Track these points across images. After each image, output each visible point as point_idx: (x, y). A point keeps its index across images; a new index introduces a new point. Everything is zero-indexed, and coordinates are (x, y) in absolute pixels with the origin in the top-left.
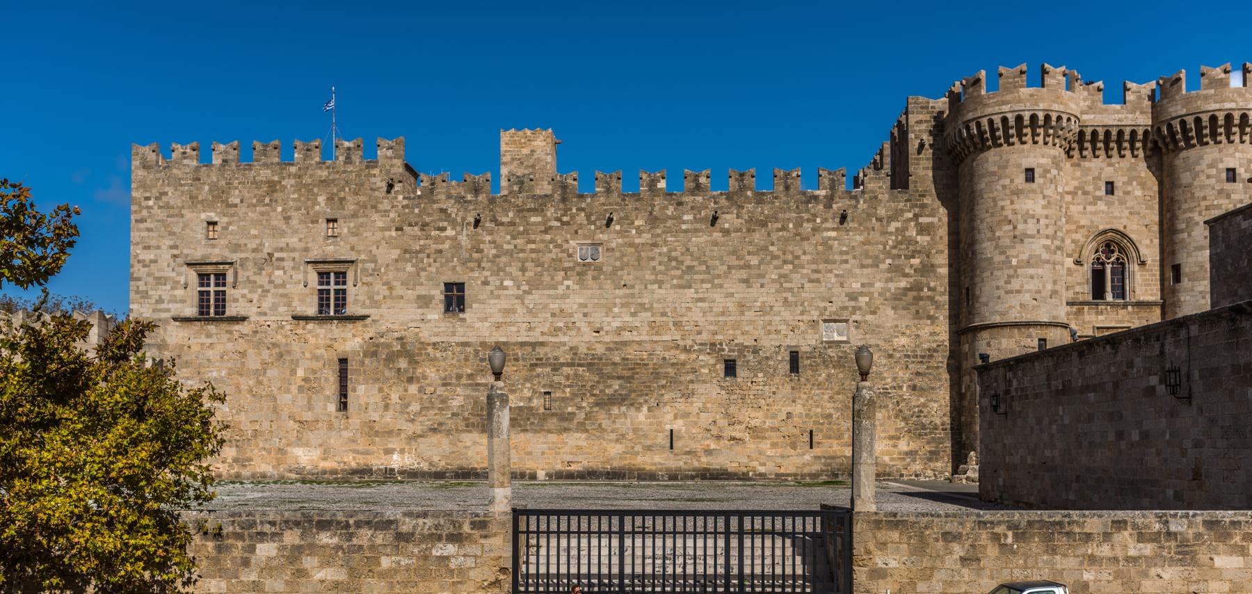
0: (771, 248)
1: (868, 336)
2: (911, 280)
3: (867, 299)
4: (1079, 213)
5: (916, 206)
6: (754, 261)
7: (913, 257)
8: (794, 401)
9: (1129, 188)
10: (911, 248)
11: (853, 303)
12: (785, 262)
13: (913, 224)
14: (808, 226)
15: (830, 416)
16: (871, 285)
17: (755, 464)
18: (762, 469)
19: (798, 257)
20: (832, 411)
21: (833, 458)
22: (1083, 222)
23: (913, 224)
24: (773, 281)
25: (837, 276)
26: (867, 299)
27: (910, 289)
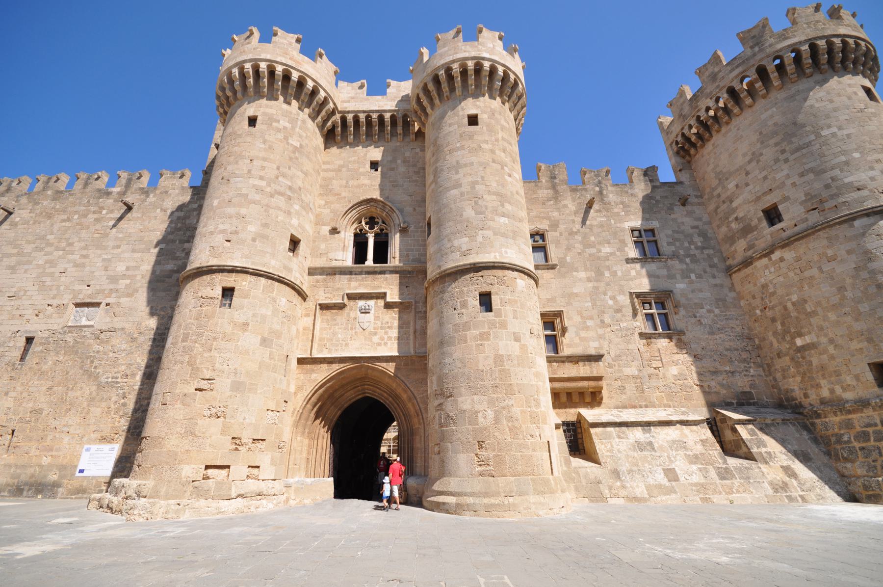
0: (49, 237)
1: (116, 319)
3: (128, 281)
4: (341, 186)
6: (28, 248)
9: (393, 165)
11: (112, 286)
12: (57, 249)
14: (91, 217)
15: (40, 411)
16: (137, 268)
19: (71, 244)
20: (44, 406)
22: (344, 194)
24: (38, 267)
25: (104, 260)
26: (128, 281)
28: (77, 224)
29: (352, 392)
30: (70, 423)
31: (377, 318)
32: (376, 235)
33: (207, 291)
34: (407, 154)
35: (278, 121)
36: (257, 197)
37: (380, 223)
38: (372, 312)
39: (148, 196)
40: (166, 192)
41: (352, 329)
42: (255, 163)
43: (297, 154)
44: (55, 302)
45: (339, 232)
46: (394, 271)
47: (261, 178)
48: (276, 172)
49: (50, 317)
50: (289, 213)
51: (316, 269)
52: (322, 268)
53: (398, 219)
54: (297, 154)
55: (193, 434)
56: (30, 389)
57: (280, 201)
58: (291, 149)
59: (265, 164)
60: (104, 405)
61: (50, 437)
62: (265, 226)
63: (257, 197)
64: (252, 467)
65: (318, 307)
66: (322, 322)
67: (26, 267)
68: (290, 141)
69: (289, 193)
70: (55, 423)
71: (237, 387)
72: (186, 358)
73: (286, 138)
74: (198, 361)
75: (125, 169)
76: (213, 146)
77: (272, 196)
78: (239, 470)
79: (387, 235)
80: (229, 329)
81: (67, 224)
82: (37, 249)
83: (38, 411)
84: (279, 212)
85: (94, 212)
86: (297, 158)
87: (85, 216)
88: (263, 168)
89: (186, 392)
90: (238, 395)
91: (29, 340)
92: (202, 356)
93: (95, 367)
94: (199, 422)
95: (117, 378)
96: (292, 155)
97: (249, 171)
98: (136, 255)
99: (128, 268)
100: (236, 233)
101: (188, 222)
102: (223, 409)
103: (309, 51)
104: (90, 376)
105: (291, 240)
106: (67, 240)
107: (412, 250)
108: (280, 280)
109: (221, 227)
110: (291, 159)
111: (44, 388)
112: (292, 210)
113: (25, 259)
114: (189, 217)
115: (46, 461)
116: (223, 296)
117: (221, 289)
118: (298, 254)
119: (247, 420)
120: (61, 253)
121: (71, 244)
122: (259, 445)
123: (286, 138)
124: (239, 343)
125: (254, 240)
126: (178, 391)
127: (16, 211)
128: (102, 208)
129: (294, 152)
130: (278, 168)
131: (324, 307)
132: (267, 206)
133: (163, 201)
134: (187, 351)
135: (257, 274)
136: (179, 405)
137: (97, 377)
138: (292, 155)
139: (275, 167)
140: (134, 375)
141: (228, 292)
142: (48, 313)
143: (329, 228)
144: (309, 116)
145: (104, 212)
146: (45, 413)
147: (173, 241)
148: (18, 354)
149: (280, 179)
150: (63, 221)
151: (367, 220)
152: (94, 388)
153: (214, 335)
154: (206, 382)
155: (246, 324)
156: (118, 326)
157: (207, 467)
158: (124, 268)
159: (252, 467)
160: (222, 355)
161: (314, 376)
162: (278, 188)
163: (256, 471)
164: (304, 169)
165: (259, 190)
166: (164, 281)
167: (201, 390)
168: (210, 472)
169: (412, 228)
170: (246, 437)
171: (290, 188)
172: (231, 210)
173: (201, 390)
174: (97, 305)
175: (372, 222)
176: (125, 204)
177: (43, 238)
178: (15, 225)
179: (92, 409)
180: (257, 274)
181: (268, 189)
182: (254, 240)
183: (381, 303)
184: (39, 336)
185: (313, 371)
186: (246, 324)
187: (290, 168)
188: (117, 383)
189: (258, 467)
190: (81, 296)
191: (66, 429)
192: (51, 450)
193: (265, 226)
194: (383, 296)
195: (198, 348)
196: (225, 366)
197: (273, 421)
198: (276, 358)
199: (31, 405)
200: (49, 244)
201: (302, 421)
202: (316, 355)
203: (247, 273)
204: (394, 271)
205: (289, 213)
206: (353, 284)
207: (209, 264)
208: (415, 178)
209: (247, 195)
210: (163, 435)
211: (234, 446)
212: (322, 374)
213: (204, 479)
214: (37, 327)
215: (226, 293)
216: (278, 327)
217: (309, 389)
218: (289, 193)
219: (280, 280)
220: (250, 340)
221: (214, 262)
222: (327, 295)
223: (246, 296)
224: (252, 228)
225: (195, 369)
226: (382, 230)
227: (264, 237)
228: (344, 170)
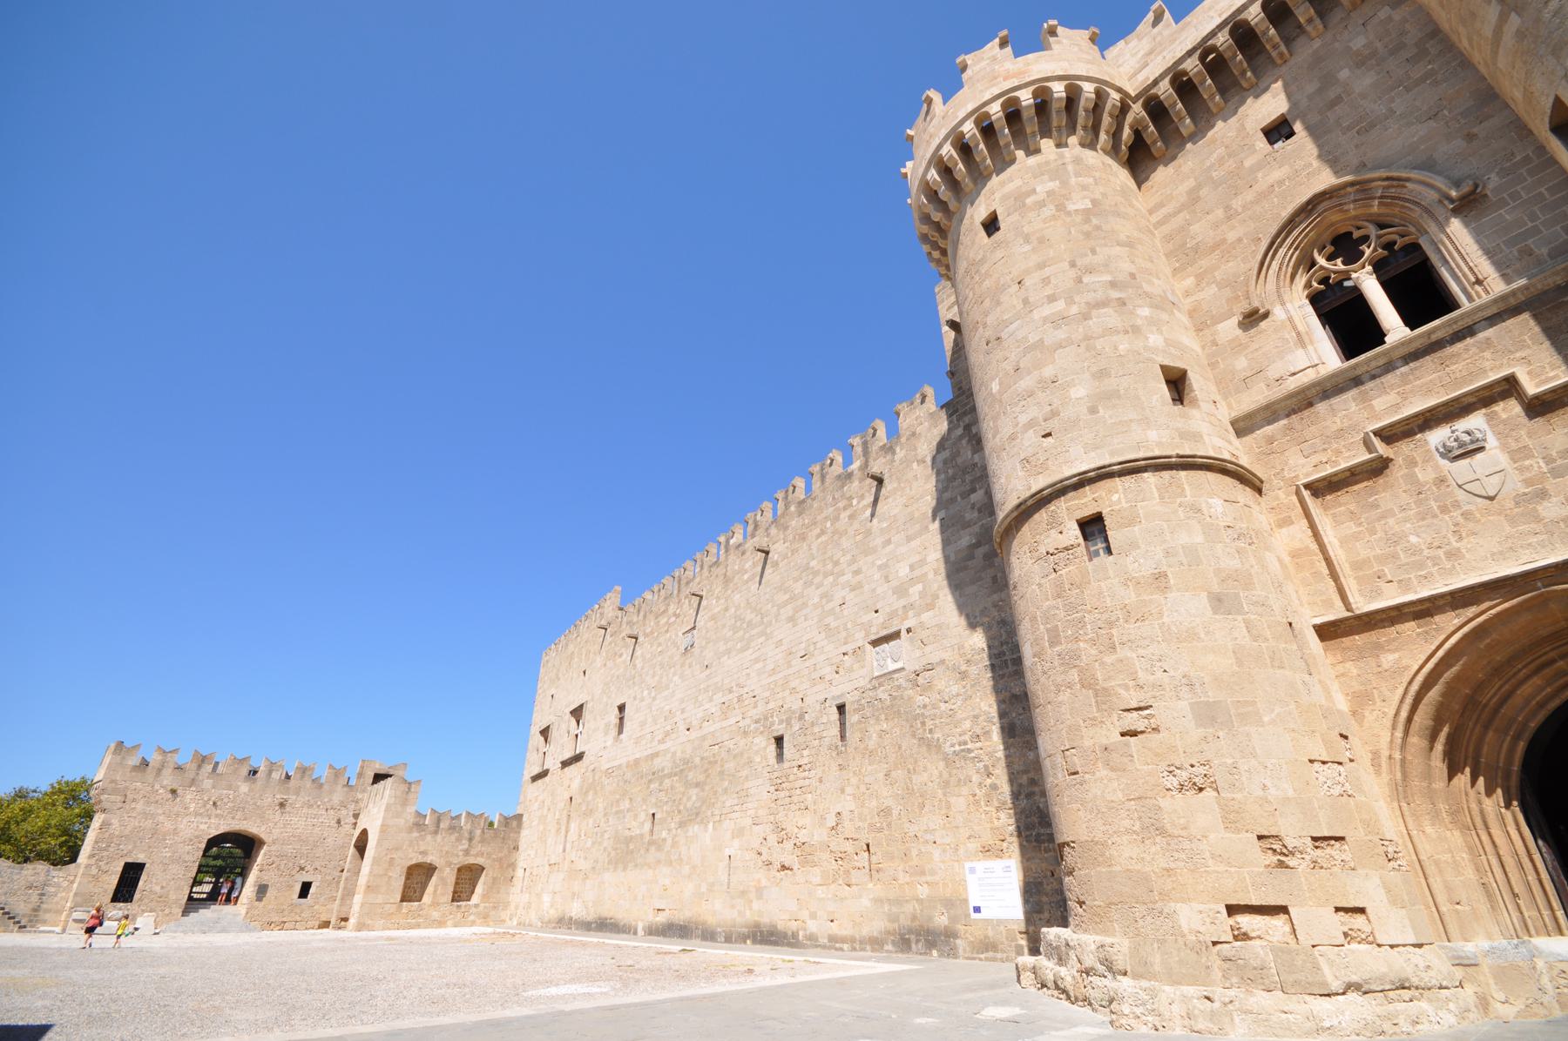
0: (813, 563)
1: (928, 649)
2: (976, 529)
3: (919, 587)
4: (1216, 226)
5: (965, 414)
7: (973, 490)
8: (843, 791)
10: (968, 478)
12: (826, 576)
13: (964, 442)
14: (844, 515)
16: (923, 562)
17: (805, 914)
18: (812, 926)
20: (890, 802)
21: (898, 902)
22: (1231, 236)
23: (964, 442)
25: (880, 567)
26: (919, 587)
27: (978, 545)
28: (834, 533)
29: (1537, 681)
30: (932, 826)
31: (1518, 454)
32: (1379, 267)
33: (1052, 540)
34: (1358, 43)
35: (1034, 191)
36: (1061, 334)
37: (1372, 231)
38: (1492, 442)
39: (894, 453)
40: (914, 434)
41: (1444, 510)
42: (1028, 282)
43: (1095, 221)
44: (849, 648)
45: (1266, 315)
46: (1503, 311)
47: (1052, 299)
48: (1072, 273)
49: (850, 670)
50: (1136, 330)
51: (1250, 416)
52: (1268, 407)
53: (1426, 188)
54: (1095, 221)
55: (1162, 831)
56: (867, 780)
57: (1108, 317)
58: (1078, 219)
59: (1047, 271)
60: (965, 790)
61: (914, 852)
62: (1102, 374)
63: (1061, 334)
64: (1347, 910)
65: (1306, 494)
66: (1337, 522)
67: (804, 612)
68: (1071, 207)
69: (1115, 294)
70: (913, 830)
71: (1208, 714)
72: (1074, 675)
73: (1061, 208)
74: (1099, 675)
75: (855, 433)
76: (946, 328)
77: (1086, 317)
78: (1316, 921)
79: (1415, 247)
80: (1130, 596)
81: (824, 538)
82: (807, 584)
83: (885, 812)
84: (1115, 338)
85: (845, 509)
86: (1098, 228)
87: (837, 518)
88: (1046, 281)
89: (1105, 742)
90: (1221, 734)
91: (841, 708)
92: (1103, 664)
93: (931, 731)
94: (1163, 803)
95: (965, 743)
96: (1086, 227)
97: (1026, 302)
98: (914, 544)
99: (912, 568)
100: (1054, 414)
101: (959, 460)
102: (1202, 770)
103: (1027, 41)
104: (929, 746)
105: (1168, 382)
106: (831, 558)
107: (1535, 231)
108: (1188, 464)
109: (1023, 419)
110: (1088, 235)
111: (881, 775)
112: (1139, 322)
113: (800, 602)
114: (958, 454)
115: (923, 891)
116: (1086, 538)
117: (1076, 526)
118: (1194, 402)
119: (1273, 791)
120: (831, 579)
121: (836, 563)
122: (1334, 850)
123: (1061, 208)
124: (1165, 619)
125: (1093, 410)
126: (1087, 743)
127: (772, 548)
128: (851, 498)
129: (1087, 221)
130: (1073, 264)
131: (1324, 488)
132: (1087, 338)
133: (916, 449)
134: (1070, 660)
135: (1131, 469)
136: (1103, 772)
137: (938, 747)
138: (1086, 227)
139: (1066, 265)
140: (987, 733)
141: (1093, 527)
142: (847, 665)
143: (1235, 320)
144: (1083, 145)
145: (855, 502)
146: (895, 812)
147: (952, 500)
148: (836, 731)
149: (1085, 280)
150: (818, 536)
151: (1330, 249)
152: (942, 764)
153: (1105, 616)
154: (1135, 714)
155: (1160, 577)
156: (935, 659)
157: (1232, 910)
158: (907, 569)
159: (1347, 910)
160: (1141, 652)
161: (1388, 659)
162: (1090, 297)
163: (1359, 920)
164: (1122, 237)
165: (1058, 321)
166: (966, 568)
167: (1134, 734)
168: (1246, 921)
169: (1493, 181)
170: (1294, 833)
171: (1113, 284)
172: (1026, 383)
173: (1134, 734)
174: (895, 635)
175: (1346, 247)
176: (873, 477)
177: (807, 568)
178: (776, 564)
179: (953, 800)
180: (1131, 469)
181: (1074, 310)
182: (1093, 410)
183: (1510, 409)
184: (849, 700)
185: (1378, 648)
186: (1160, 577)
187: (1094, 252)
188: (969, 751)
189: (1362, 911)
190: (874, 630)
191: (929, 837)
192: (923, 873)
193: (1102, 374)
194: (1509, 387)
195: (1087, 652)
196: (1159, 674)
197: (1337, 790)
198: (1268, 634)
199: (874, 803)
200: (816, 573)
201: (1416, 783)
202: (1363, 605)
203: (1111, 475)
204: (1503, 311)
205: (1136, 330)
206: (1380, 403)
207: (1034, 490)
208: (1417, 72)
209: (1041, 340)
210: (1099, 836)
211: (1275, 858)
212: (1412, 652)
213: (1236, 938)
214: (843, 689)
215: (1088, 530)
216: (1234, 563)
217: (1391, 699)
218: (1115, 294)
219: (1188, 464)
220: (1186, 607)
221: (1040, 483)
222: (1314, 459)
223: (1132, 521)
224: (1079, 392)
225: (1104, 696)
226: (1389, 246)
227: (1110, 396)
228: (1203, 192)
